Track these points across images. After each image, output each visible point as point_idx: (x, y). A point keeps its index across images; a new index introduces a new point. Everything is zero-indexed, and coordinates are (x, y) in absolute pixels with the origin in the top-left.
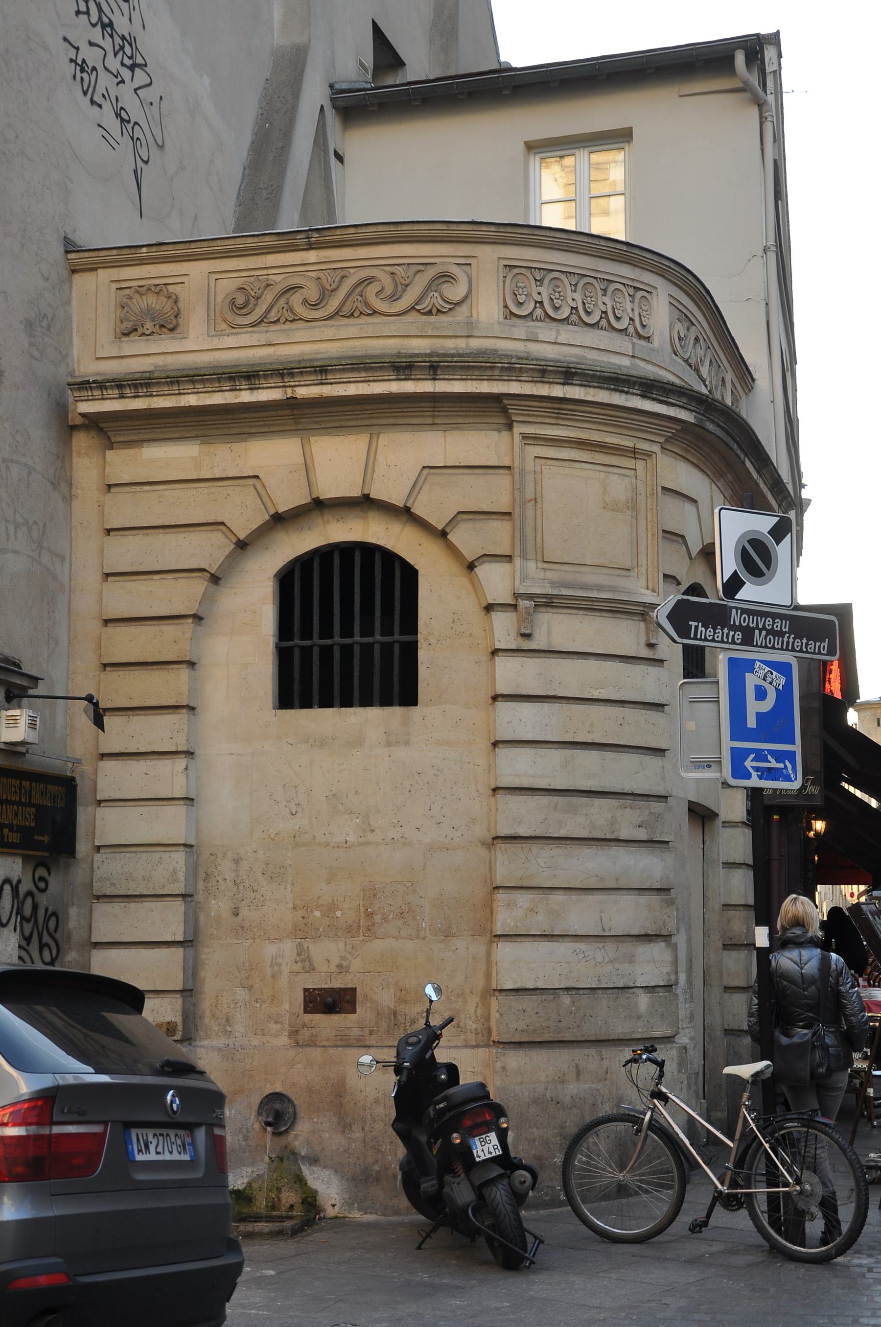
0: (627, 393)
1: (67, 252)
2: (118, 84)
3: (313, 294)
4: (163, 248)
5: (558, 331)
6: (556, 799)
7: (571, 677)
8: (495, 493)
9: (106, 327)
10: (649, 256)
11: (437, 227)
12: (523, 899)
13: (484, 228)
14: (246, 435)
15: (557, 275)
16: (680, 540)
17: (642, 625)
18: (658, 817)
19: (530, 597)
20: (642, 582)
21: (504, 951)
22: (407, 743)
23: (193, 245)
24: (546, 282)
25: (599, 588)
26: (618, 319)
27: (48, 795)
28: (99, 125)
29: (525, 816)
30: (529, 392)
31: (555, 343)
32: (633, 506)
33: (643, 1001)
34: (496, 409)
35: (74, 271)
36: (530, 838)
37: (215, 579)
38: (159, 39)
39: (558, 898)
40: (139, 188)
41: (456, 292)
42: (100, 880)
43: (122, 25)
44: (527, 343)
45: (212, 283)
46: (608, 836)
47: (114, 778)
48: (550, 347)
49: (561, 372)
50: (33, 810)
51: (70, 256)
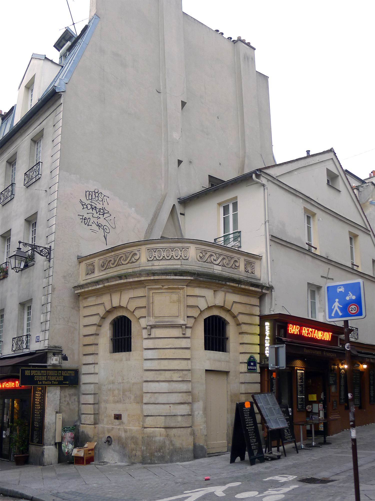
3: (113, 262)
9: (84, 274)
12: (149, 395)
14: (103, 294)
18: (185, 375)
19: (150, 326)
21: (145, 407)
29: (150, 376)
32: (179, 301)
33: (179, 418)
34: (140, 284)
38: (114, 204)
43: (99, 206)
47: (84, 369)
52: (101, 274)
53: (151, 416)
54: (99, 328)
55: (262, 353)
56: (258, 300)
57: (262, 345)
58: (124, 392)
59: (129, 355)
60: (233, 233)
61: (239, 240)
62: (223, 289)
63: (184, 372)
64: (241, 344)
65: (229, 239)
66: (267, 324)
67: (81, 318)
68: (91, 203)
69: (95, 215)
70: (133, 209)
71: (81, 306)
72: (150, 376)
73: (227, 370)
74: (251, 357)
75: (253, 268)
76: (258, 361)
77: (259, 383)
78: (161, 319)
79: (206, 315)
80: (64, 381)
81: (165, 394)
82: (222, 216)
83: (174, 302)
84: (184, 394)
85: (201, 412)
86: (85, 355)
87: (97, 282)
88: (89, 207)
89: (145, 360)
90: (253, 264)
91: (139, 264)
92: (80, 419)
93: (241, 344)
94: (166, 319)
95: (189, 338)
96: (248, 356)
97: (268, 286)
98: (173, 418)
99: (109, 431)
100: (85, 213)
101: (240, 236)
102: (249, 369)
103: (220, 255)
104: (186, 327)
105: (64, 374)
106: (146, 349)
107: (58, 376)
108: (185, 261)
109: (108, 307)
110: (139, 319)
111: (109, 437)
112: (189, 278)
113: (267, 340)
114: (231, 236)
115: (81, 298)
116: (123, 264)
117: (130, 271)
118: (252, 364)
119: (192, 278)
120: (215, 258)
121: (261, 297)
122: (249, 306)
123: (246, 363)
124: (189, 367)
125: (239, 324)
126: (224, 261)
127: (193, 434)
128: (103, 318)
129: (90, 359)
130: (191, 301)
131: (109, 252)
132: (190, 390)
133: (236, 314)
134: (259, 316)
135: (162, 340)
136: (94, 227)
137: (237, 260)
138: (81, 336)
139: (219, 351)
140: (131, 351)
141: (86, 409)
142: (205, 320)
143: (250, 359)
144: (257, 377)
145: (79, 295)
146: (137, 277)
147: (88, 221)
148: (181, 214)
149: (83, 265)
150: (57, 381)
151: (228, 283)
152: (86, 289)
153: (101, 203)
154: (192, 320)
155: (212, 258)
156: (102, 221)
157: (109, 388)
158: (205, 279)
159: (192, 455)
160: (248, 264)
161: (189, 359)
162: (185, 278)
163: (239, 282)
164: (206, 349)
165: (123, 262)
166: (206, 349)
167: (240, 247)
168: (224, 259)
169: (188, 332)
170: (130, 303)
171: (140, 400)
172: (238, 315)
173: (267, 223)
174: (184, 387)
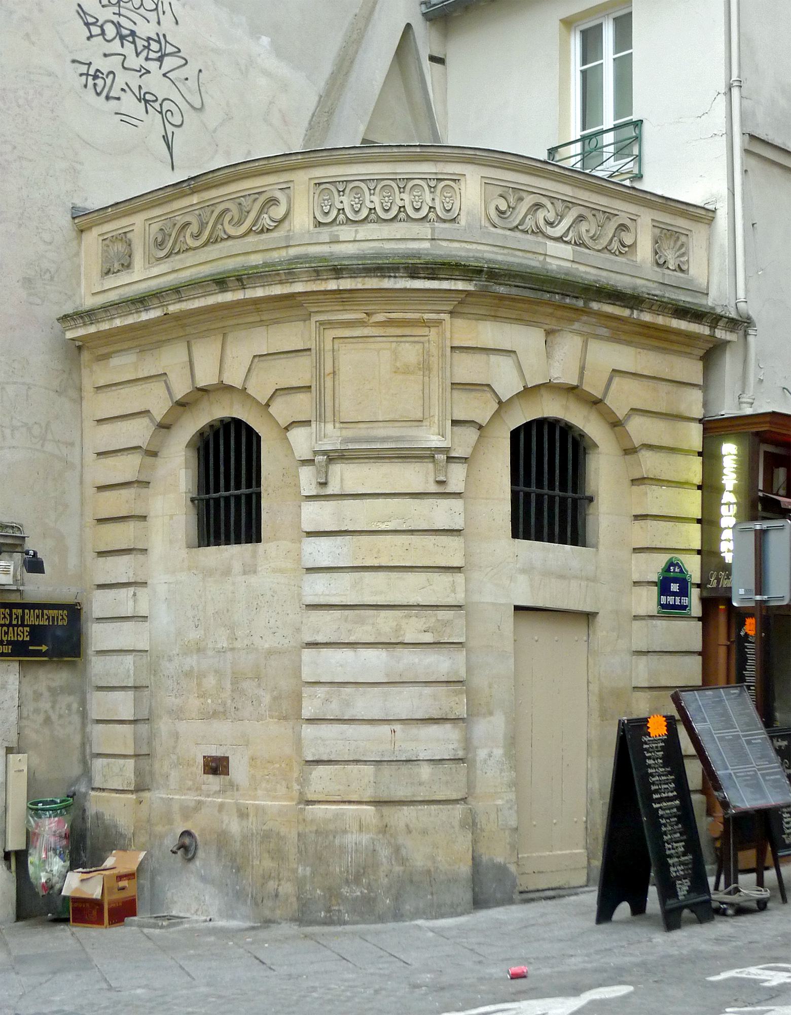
0: (395, 277)
1: (74, 218)
2: (140, 76)
3: (194, 228)
4: (119, 206)
5: (356, 231)
6: (347, 612)
7: (359, 514)
8: (298, 372)
9: (96, 269)
10: (448, 151)
11: (261, 163)
12: (321, 691)
13: (294, 158)
15: (356, 184)
16: (486, 388)
17: (431, 466)
18: (446, 623)
19: (324, 452)
20: (435, 429)
21: (308, 731)
22: (255, 572)
23: (133, 202)
24: (347, 191)
25: (384, 440)
26: (417, 210)
27: (46, 617)
28: (117, 113)
29: (326, 626)
30: (309, 290)
31: (355, 241)
32: (425, 367)
33: (425, 771)
35: (82, 231)
36: (326, 644)
37: (153, 454)
38: (195, 23)
39: (349, 690)
40: (170, 148)
41: (278, 212)
42: (95, 675)
44: (331, 245)
45: (147, 228)
46: (393, 641)
47: (99, 604)
48: (350, 245)
49: (331, 270)
50: (28, 629)
51: (76, 221)
52: (156, 271)
53: (329, 762)
54: (150, 460)
55: (708, 552)
56: (700, 365)
57: (708, 521)
58: (235, 681)
59: (254, 555)
60: (616, 128)
61: (636, 151)
62: (576, 326)
63: (442, 614)
64: (637, 517)
65: (599, 148)
66: (730, 451)
67: (89, 424)
68: (115, 18)
69: (134, 62)
70: (265, 40)
71: (88, 385)
72: (326, 626)
73: (588, 609)
74: (671, 564)
75: (683, 250)
76: (696, 577)
77: (700, 654)
78: (362, 431)
79: (519, 417)
80: (31, 643)
81: (376, 690)
82: (576, 67)
83: (406, 371)
84: (442, 690)
85: (499, 752)
86: (101, 554)
87: (141, 302)
88: (111, 31)
89: (310, 570)
90: (683, 239)
91: (288, 238)
92: (87, 772)
93: (637, 517)
94: (381, 432)
95: (457, 495)
96: (661, 560)
97: (733, 315)
98: (404, 769)
99: (187, 812)
100: (95, 53)
101: (638, 139)
102: (663, 606)
103: (569, 204)
104: (450, 459)
105: (31, 618)
106: (310, 534)
107: (10, 625)
108: (447, 225)
109: (181, 389)
110: (287, 429)
111: (187, 833)
112: (460, 285)
113: (729, 504)
114: (609, 138)
115: (86, 356)
116: (229, 237)
117: (256, 260)
118: (675, 587)
119: (470, 287)
120: (551, 216)
121: (711, 354)
122: (664, 387)
123: (655, 584)
124: (459, 597)
125: (630, 451)
126: (583, 227)
127: (471, 823)
128: (165, 426)
129: (120, 569)
130: (468, 369)
131: (184, 195)
132: (462, 674)
133: (621, 413)
134: (700, 421)
135: (368, 502)
136: (130, 104)
137: (628, 222)
138: (90, 491)
139: (563, 541)
140: (259, 540)
141: (107, 739)
142: (515, 435)
143: (667, 570)
144: (689, 633)
145: (79, 346)
146: (281, 282)
147: (109, 81)
148: (433, 59)
149: (92, 238)
150: (9, 643)
151: (595, 306)
152: (105, 326)
153: (152, 16)
154: (471, 435)
155: (541, 215)
156: (155, 84)
157: (187, 668)
158: (514, 291)
159: (467, 896)
160: (665, 236)
161: (459, 569)
162: (445, 285)
163: (632, 300)
164: (515, 535)
165: (232, 231)
166: (515, 535)
167: (639, 177)
168: (581, 218)
169: (457, 477)
170: (254, 374)
171: (290, 710)
172: (628, 416)
173: (735, 92)
174: (441, 664)
